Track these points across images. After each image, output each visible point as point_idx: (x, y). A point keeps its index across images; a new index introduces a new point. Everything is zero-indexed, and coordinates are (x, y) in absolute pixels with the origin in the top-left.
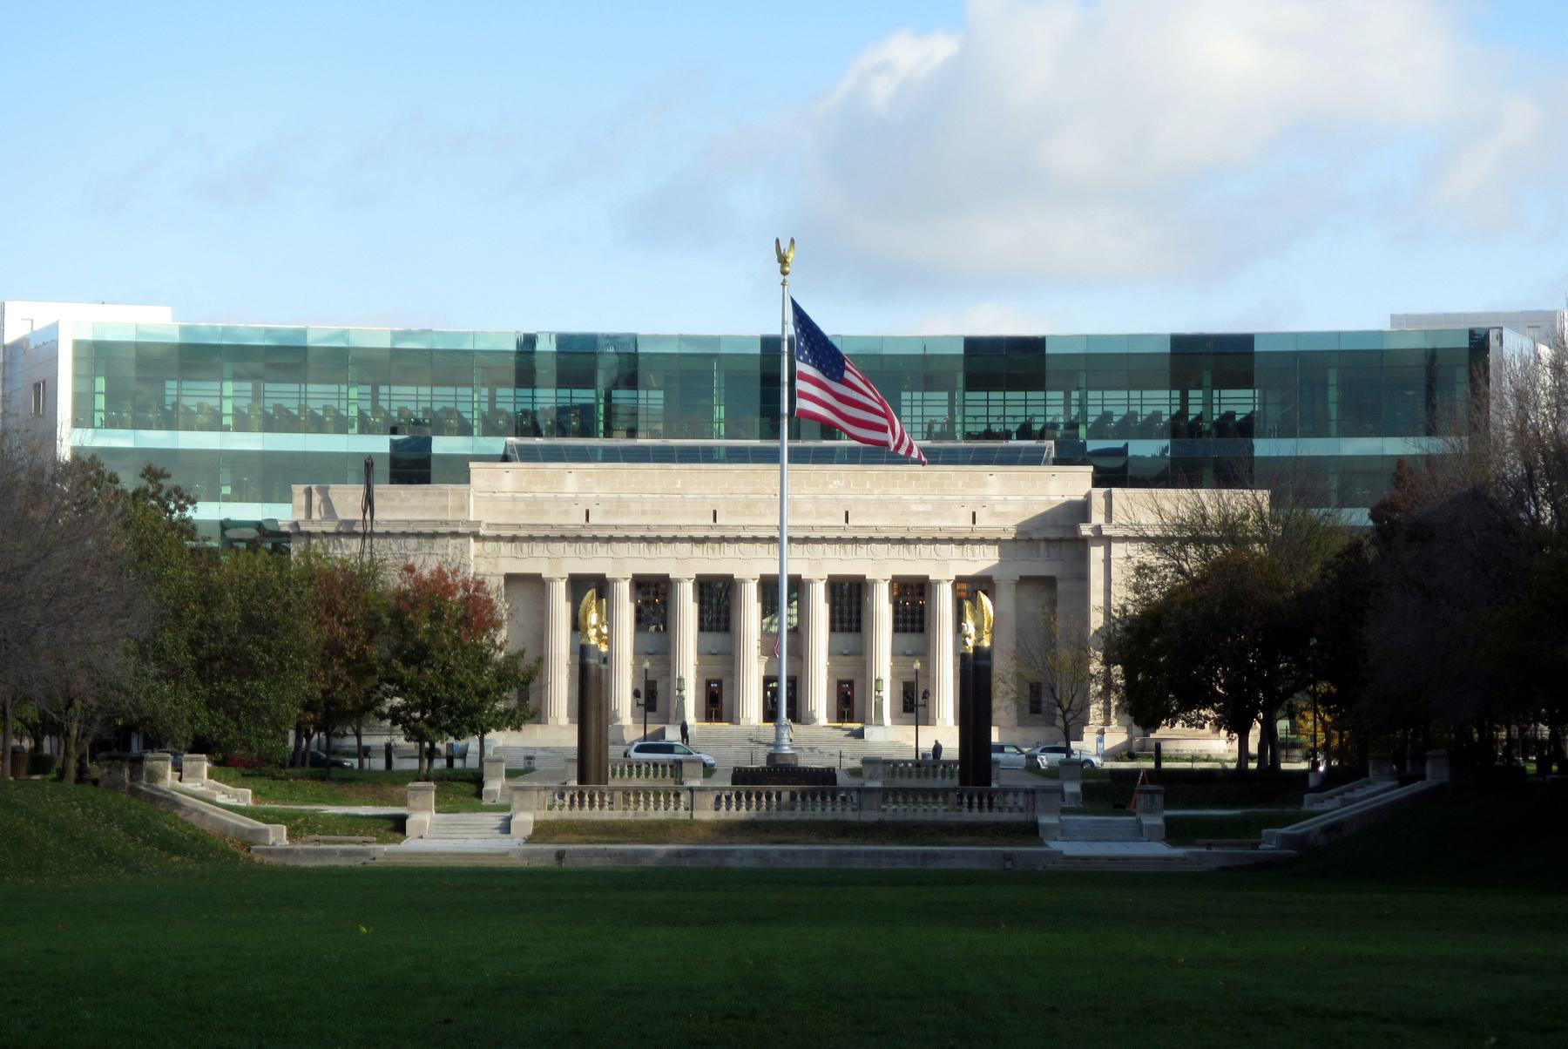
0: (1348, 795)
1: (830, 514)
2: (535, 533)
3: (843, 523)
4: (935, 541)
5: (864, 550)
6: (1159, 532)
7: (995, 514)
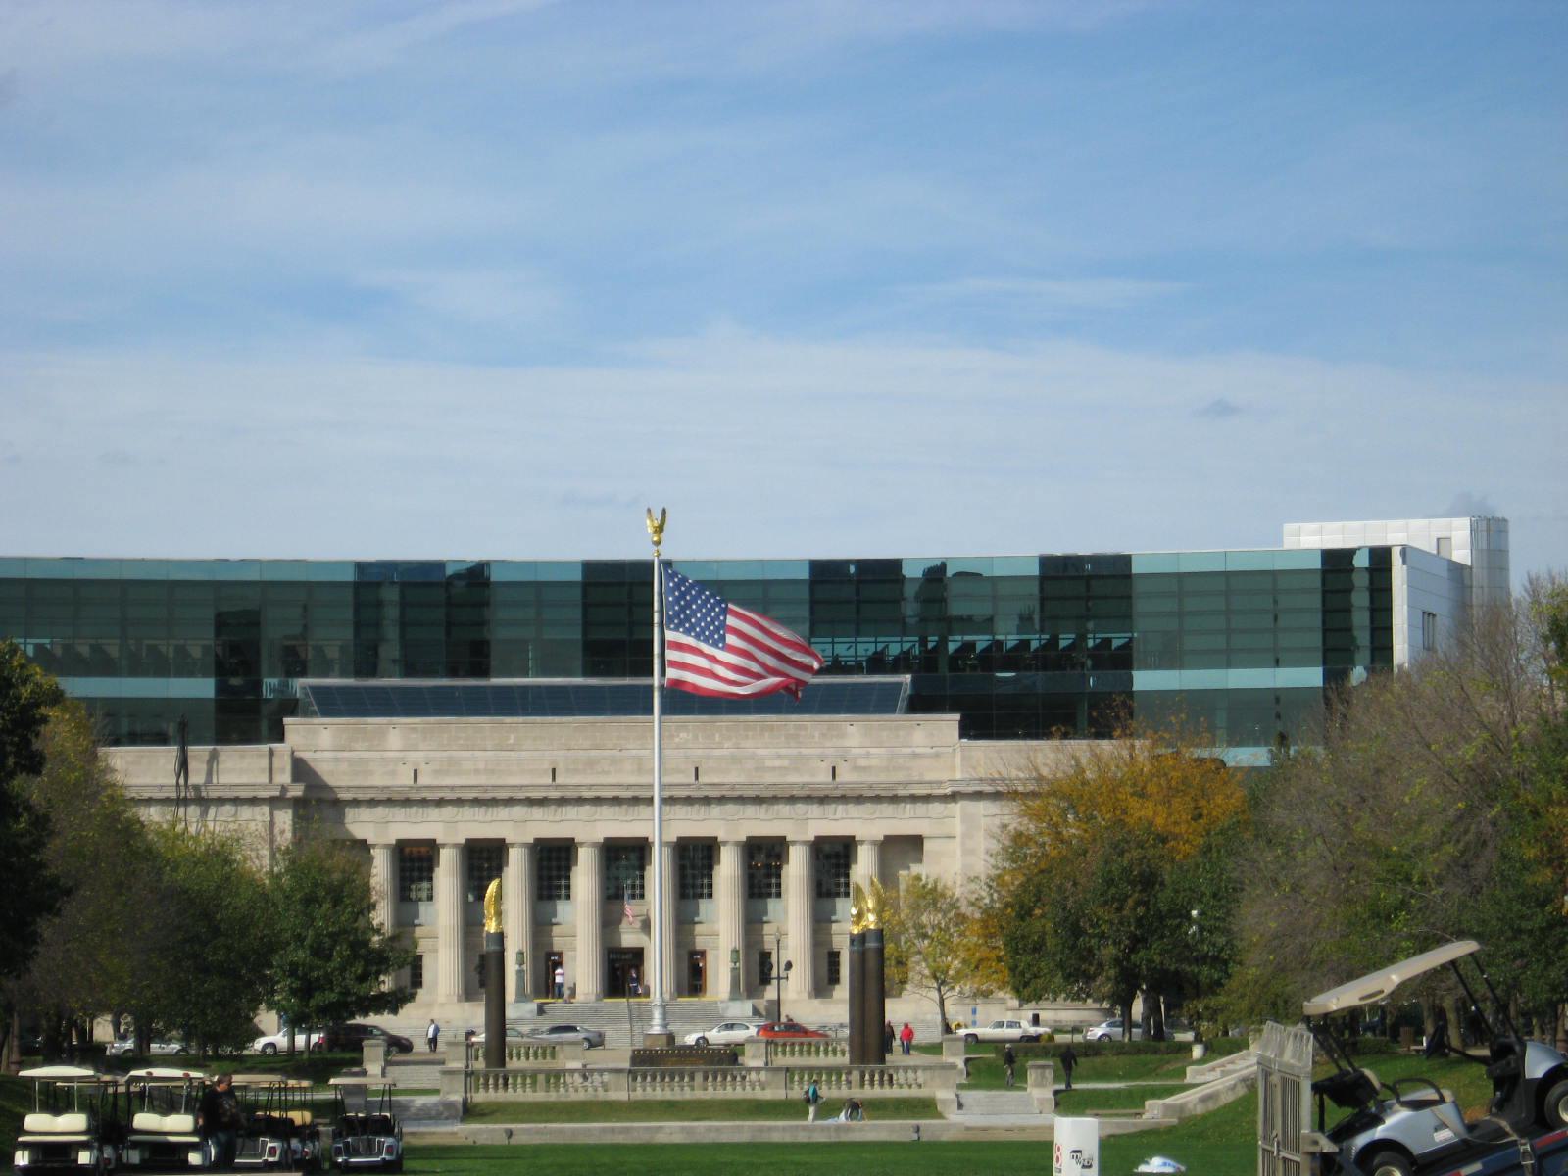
0: (1230, 1067)
1: (679, 771)
2: (360, 796)
3: (692, 779)
4: (792, 799)
5: (716, 810)
6: (1031, 787)
7: (856, 769)
